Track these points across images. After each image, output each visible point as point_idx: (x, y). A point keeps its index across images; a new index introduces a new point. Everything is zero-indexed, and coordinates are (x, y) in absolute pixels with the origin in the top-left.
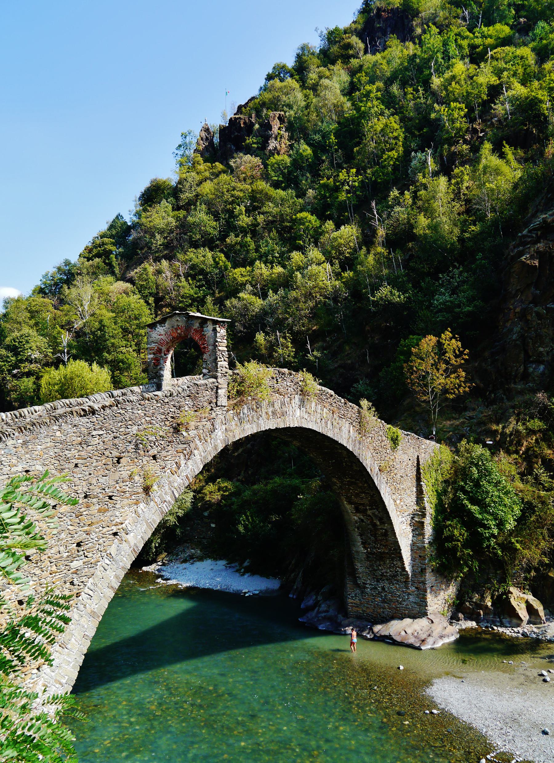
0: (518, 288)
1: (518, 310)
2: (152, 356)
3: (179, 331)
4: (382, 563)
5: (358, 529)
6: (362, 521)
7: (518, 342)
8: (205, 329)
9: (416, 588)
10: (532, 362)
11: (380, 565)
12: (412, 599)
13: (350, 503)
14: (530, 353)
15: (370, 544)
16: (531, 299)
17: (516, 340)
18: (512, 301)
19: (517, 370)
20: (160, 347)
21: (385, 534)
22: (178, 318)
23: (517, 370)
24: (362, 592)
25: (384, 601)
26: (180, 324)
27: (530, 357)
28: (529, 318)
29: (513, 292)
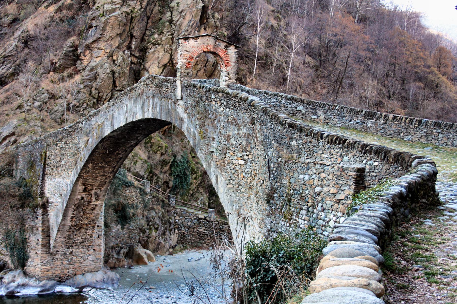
0: (111, 35)
1: (108, 51)
2: (185, 61)
3: (209, 48)
4: (78, 233)
5: (75, 205)
6: (82, 198)
7: (110, 75)
8: (228, 51)
9: (94, 250)
10: (117, 91)
11: (75, 235)
12: (90, 258)
13: (83, 184)
14: (117, 84)
15: (78, 217)
16: (117, 45)
17: (109, 73)
18: (105, 43)
19: (107, 95)
20: (192, 55)
21: (93, 209)
22: (208, 39)
23: (107, 95)
24: (53, 259)
25: (70, 264)
26: (210, 43)
27: (117, 87)
28: (115, 58)
29: (107, 37)
